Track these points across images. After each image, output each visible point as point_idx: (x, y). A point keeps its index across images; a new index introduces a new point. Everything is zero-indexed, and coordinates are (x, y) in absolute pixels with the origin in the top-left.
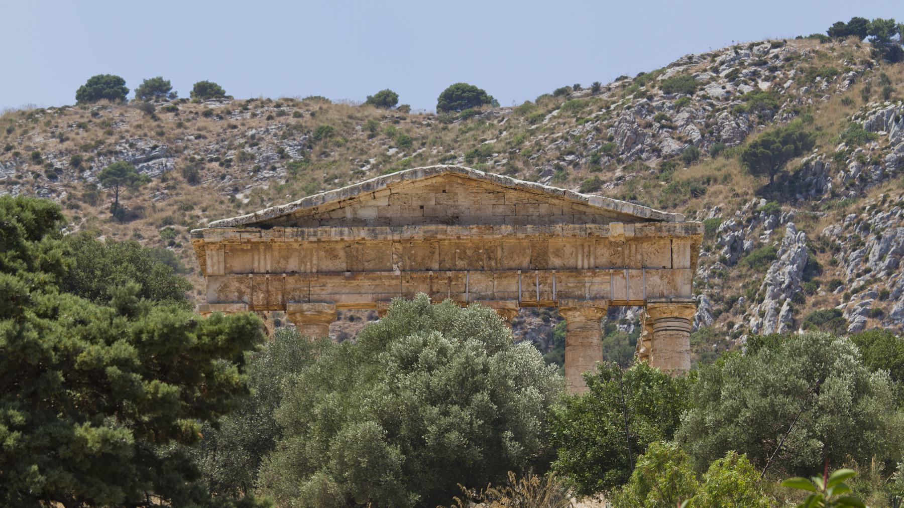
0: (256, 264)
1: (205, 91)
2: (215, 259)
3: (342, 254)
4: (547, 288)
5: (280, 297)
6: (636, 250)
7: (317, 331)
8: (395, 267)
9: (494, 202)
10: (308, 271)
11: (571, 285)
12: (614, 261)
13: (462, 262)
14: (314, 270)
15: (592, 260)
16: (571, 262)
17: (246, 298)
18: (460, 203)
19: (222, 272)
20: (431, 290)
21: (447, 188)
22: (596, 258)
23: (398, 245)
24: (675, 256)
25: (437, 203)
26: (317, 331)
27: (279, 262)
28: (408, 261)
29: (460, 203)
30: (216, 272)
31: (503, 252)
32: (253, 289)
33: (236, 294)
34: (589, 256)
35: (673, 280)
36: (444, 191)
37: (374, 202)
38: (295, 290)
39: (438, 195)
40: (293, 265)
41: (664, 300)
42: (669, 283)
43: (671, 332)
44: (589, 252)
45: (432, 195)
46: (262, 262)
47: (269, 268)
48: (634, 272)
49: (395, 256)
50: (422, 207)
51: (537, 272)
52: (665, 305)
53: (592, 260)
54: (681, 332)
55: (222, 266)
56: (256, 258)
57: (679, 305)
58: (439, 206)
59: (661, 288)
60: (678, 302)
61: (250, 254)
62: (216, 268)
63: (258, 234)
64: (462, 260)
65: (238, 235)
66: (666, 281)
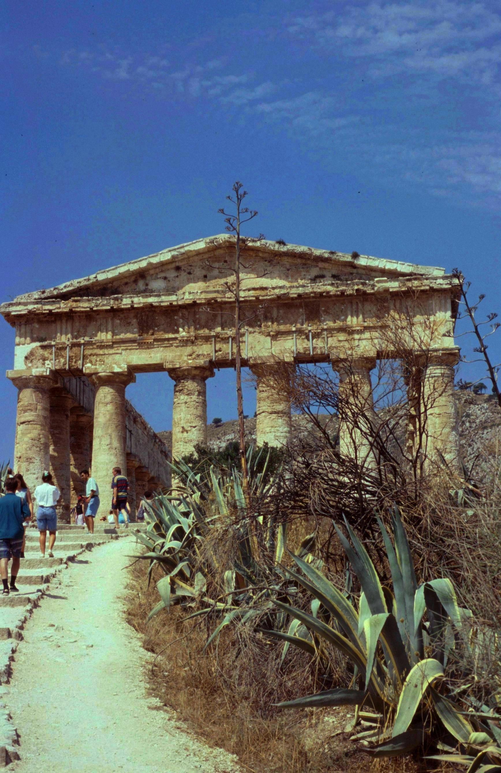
6: (401, 304)
31: (278, 312)
33: (41, 361)
37: (163, 275)
44: (357, 308)
63: (58, 306)
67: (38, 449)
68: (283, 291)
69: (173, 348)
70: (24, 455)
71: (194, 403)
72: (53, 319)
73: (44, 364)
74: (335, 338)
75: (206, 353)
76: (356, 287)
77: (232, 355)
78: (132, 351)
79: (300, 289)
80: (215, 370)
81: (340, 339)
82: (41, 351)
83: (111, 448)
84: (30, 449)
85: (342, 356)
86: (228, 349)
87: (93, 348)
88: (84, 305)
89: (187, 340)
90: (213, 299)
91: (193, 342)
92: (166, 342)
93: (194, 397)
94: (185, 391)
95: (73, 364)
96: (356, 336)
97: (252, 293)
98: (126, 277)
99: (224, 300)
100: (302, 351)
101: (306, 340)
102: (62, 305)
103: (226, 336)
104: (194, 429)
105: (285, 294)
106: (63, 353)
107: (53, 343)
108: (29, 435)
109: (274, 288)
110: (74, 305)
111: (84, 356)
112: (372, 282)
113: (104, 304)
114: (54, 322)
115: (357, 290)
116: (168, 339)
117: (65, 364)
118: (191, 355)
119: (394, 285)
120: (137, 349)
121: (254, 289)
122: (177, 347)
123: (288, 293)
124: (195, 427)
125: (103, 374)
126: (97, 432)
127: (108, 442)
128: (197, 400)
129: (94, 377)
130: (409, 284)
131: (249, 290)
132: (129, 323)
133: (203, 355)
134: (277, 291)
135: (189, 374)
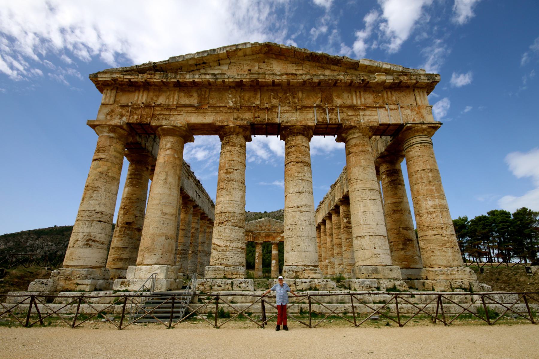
0: (136, 99)
2: (108, 95)
3: (195, 95)
4: (334, 117)
5: (149, 119)
6: (391, 94)
7: (172, 140)
8: (230, 101)
9: (296, 68)
10: (171, 103)
11: (350, 114)
13: (275, 100)
14: (175, 103)
15: (363, 100)
16: (348, 102)
17: (124, 119)
18: (274, 68)
19: (111, 102)
20: (254, 116)
21: (266, 61)
22: (365, 99)
23: (232, 90)
24: (418, 98)
26: (172, 140)
27: (152, 99)
28: (239, 98)
29: (274, 68)
30: (107, 103)
33: (119, 116)
34: (360, 97)
35: (420, 112)
36: (264, 62)
37: (219, 67)
38: (159, 114)
39: (260, 64)
40: (161, 100)
41: (418, 122)
42: (417, 113)
43: (425, 144)
46: (140, 97)
47: (144, 101)
48: (393, 107)
49: (230, 96)
50: (249, 70)
51: (326, 105)
53: (363, 100)
56: (137, 95)
58: (260, 70)
59: (413, 117)
60: (429, 124)
61: (133, 94)
62: (107, 100)
63: (136, 77)
64: (275, 99)
65: (122, 75)
66: (415, 113)
67: (105, 181)
68: (308, 77)
69: (223, 114)
70: (91, 185)
71: (237, 152)
72: (134, 89)
73: (120, 119)
74: (345, 114)
75: (247, 118)
76: (362, 78)
77: (268, 120)
78: (192, 114)
79: (321, 77)
80: (253, 137)
81: (349, 114)
82: (120, 110)
83: (165, 183)
84: (97, 180)
85: (353, 124)
86: (265, 117)
87: (162, 110)
88: (157, 78)
89: (234, 108)
90: (256, 79)
91: (238, 110)
92: (218, 109)
93: (237, 148)
94: (231, 143)
95: (144, 120)
96: (361, 113)
97: (284, 77)
98: (191, 65)
99: (263, 80)
100: (321, 120)
101: (323, 114)
102: (140, 76)
103: (264, 107)
104: (235, 172)
105: (309, 79)
106: (137, 112)
107: (130, 104)
108: (98, 169)
109: (301, 75)
110: (149, 76)
111: (153, 115)
112: (373, 76)
113: (172, 78)
114: (134, 91)
115: (363, 80)
116: (220, 107)
117: (137, 120)
118: (236, 119)
119: (389, 79)
120: (195, 113)
121: (286, 74)
122: (226, 113)
123: (312, 79)
124: (237, 170)
125: (166, 127)
126: (157, 170)
127: (164, 178)
128: (240, 151)
129: (159, 129)
130: (401, 78)
131: (282, 75)
132: (191, 96)
133: (246, 119)
134: (304, 77)
135: (234, 131)
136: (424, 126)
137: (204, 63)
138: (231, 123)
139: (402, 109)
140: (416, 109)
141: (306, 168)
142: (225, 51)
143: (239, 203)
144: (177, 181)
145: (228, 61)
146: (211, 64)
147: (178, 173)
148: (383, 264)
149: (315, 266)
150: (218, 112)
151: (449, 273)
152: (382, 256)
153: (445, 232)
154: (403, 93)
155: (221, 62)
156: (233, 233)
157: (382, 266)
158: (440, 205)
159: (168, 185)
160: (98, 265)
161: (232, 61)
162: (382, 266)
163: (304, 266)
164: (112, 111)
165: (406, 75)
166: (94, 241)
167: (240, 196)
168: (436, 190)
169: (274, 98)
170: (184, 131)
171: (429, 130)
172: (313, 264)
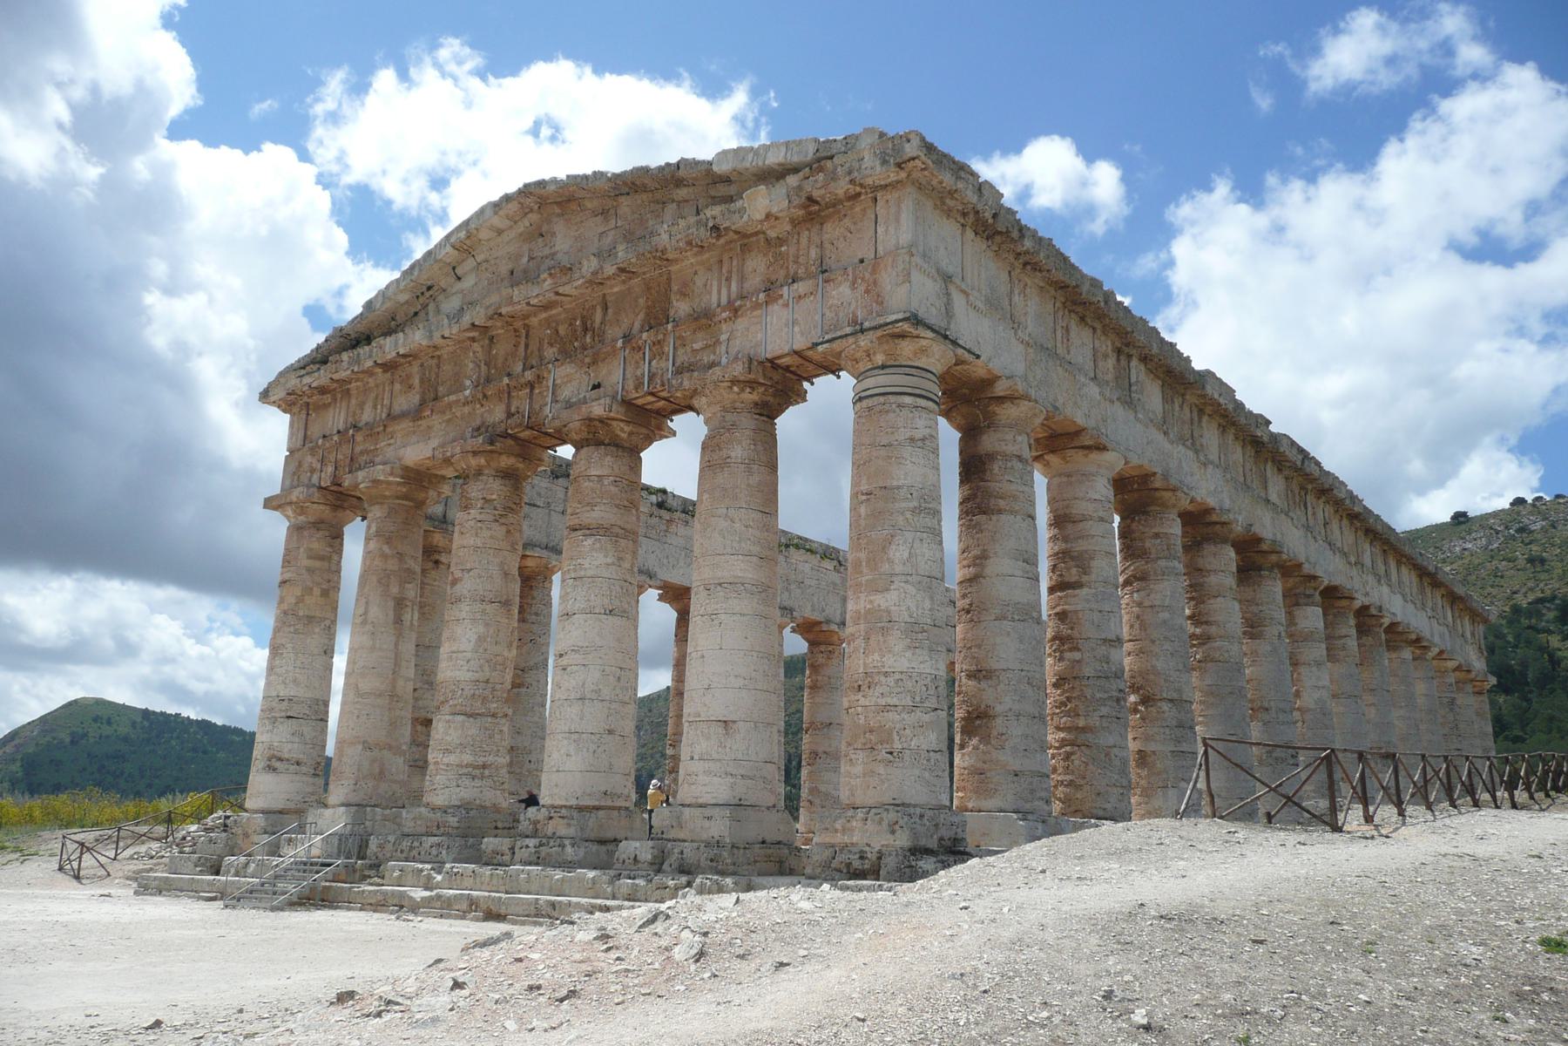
1: (1558, 496)
12: (773, 278)
21: (544, 229)
22: (742, 279)
25: (531, 258)
32: (322, 461)
34: (728, 279)
35: (875, 282)
38: (362, 453)
40: (367, 416)
42: (867, 291)
45: (526, 247)
48: (801, 287)
52: (851, 340)
54: (892, 398)
55: (301, 435)
57: (879, 333)
66: (863, 288)
81: (696, 346)
82: (309, 459)
99: (509, 309)
103: (523, 381)
136: (864, 341)
137: (429, 288)
138: (458, 450)
139: (829, 287)
140: (867, 275)
141: (590, 541)
142: (449, 249)
143: (469, 655)
144: (391, 613)
145: (470, 263)
146: (443, 284)
147: (395, 590)
148: (700, 801)
149: (580, 809)
150: (449, 421)
151: (838, 826)
152: (702, 778)
153: (863, 701)
154: (847, 222)
155: (459, 271)
156: (451, 731)
157: (701, 806)
158: (868, 612)
159: (369, 627)
160: (292, 806)
161: (480, 258)
162: (701, 806)
163: (553, 807)
164: (300, 464)
165: (821, 169)
166: (280, 759)
167: (474, 638)
168: (868, 561)
169: (551, 345)
170: (399, 484)
171: (886, 347)
172: (573, 802)
